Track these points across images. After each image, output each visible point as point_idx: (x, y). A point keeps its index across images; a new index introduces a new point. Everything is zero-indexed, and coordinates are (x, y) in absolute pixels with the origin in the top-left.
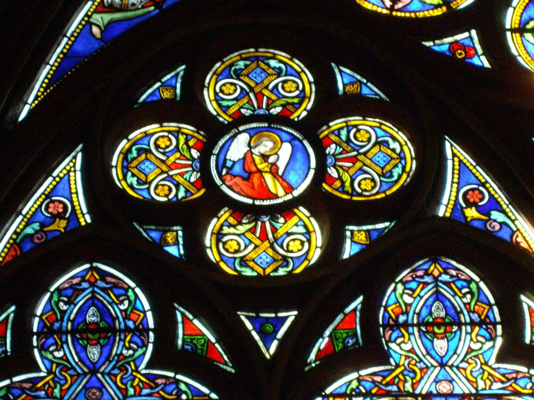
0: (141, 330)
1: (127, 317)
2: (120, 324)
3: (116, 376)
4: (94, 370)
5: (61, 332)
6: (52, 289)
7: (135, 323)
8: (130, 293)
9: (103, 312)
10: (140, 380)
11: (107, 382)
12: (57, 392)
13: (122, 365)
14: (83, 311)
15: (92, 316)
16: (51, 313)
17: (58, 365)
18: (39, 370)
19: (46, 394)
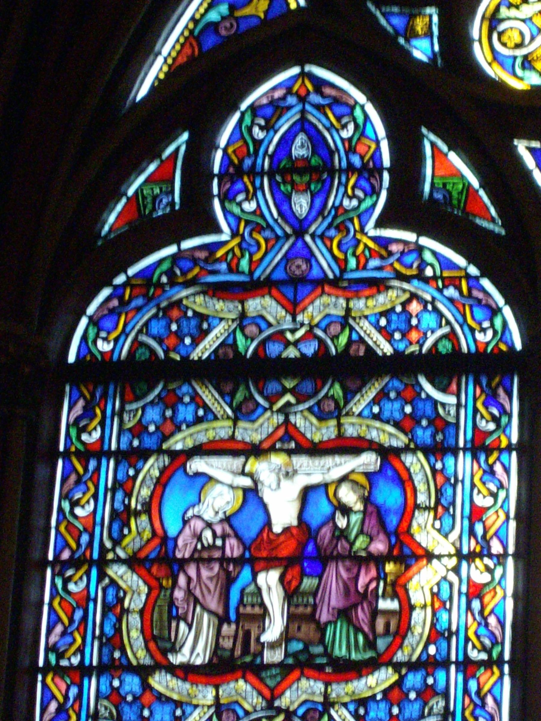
0: (370, 171)
1: (351, 150)
2: (340, 161)
3: (331, 239)
4: (300, 228)
5: (253, 172)
6: (244, 106)
7: (362, 158)
8: (358, 112)
9: (317, 141)
10: (366, 246)
11: (318, 249)
12: (244, 264)
13: (343, 222)
14: (287, 141)
15: (300, 148)
16: (240, 144)
17: (247, 222)
18: (218, 230)
19: (229, 265)
